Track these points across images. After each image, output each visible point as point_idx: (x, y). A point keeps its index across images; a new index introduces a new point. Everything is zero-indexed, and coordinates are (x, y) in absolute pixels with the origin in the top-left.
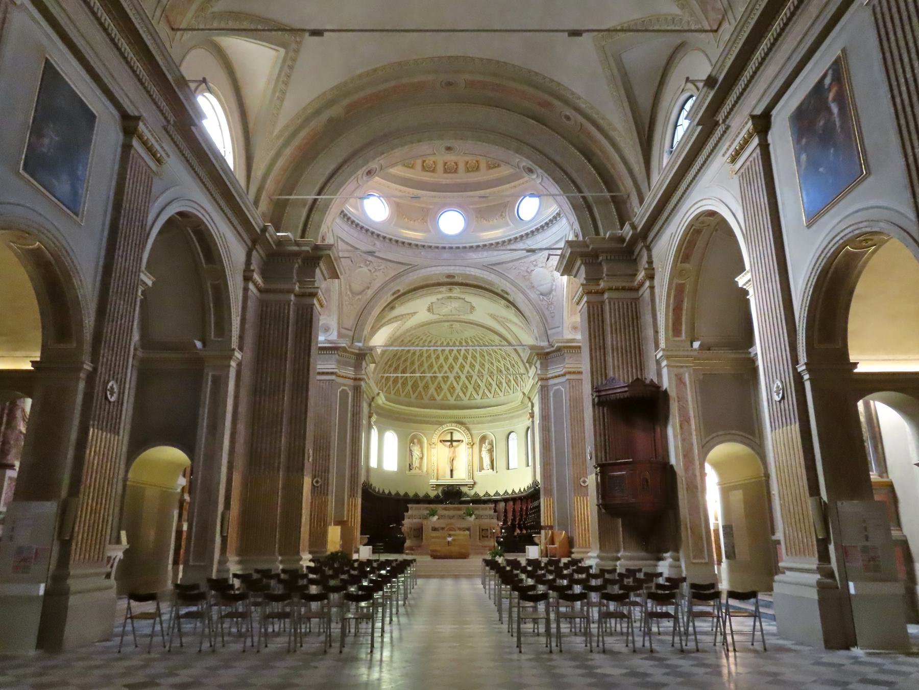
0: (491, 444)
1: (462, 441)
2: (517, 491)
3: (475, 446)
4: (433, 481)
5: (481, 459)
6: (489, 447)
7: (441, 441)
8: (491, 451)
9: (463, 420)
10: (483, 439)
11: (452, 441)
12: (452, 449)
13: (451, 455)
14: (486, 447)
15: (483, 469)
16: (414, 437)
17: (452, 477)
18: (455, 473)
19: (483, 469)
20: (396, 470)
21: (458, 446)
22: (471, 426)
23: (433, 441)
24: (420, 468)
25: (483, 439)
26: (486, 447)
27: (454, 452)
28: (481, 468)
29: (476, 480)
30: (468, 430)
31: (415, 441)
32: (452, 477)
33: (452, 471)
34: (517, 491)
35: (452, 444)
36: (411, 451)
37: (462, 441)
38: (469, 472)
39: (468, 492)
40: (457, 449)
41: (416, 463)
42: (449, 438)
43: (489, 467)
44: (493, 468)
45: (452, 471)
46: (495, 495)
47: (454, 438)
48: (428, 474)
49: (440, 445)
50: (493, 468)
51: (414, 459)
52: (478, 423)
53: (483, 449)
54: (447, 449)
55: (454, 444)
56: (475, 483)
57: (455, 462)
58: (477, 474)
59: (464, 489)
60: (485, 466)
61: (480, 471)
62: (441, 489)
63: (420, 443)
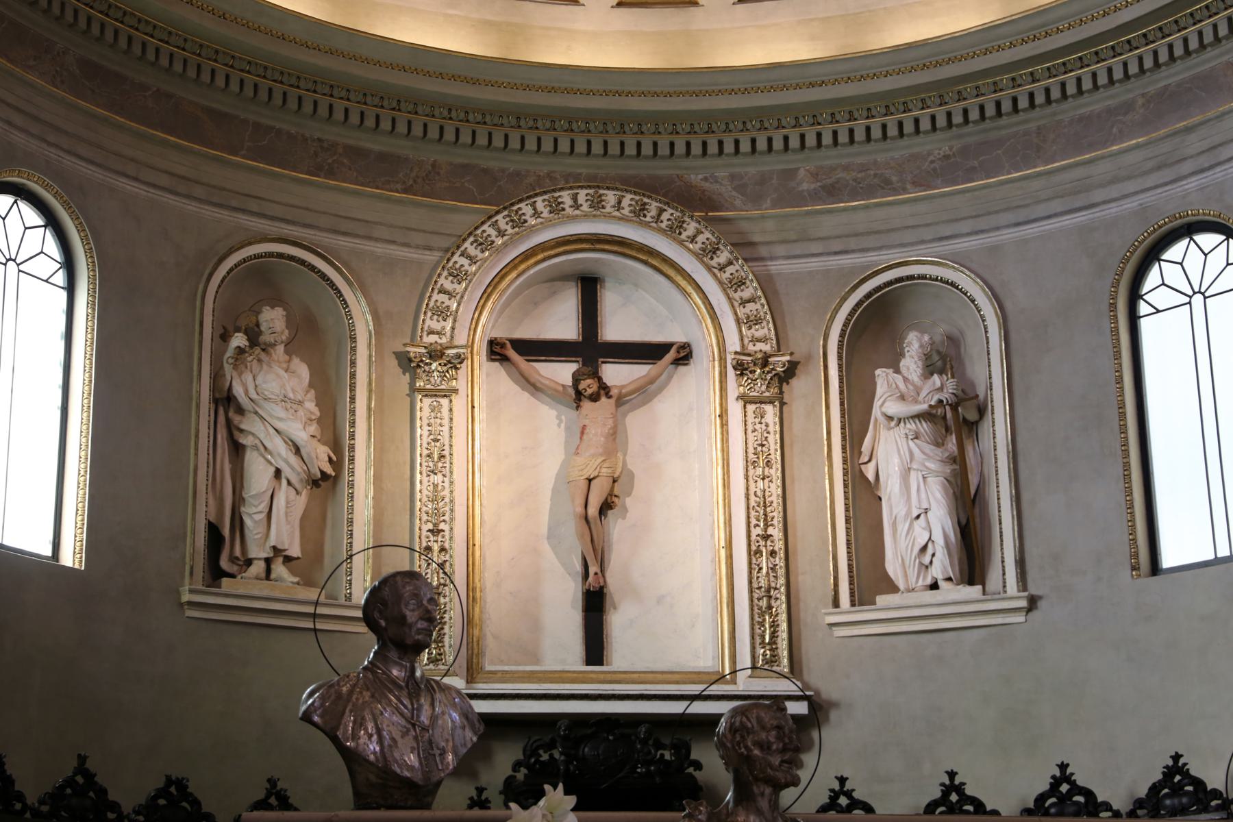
1: (684, 355)
3: (798, 385)
7: (496, 350)
9: (696, 174)
12: (598, 414)
13: (589, 463)
15: (891, 587)
17: (595, 649)
18: (617, 622)
19: (891, 587)
20: (69, 557)
21: (644, 393)
27: (616, 437)
30: (745, 247)
31: (273, 320)
32: (595, 649)
36: (225, 401)
37: (684, 355)
40: (635, 421)
43: (941, 566)
47: (614, 329)
51: (258, 475)
52: (832, 192)
53: (886, 403)
55: (616, 374)
56: (819, 710)
57: (618, 529)
61: (861, 598)
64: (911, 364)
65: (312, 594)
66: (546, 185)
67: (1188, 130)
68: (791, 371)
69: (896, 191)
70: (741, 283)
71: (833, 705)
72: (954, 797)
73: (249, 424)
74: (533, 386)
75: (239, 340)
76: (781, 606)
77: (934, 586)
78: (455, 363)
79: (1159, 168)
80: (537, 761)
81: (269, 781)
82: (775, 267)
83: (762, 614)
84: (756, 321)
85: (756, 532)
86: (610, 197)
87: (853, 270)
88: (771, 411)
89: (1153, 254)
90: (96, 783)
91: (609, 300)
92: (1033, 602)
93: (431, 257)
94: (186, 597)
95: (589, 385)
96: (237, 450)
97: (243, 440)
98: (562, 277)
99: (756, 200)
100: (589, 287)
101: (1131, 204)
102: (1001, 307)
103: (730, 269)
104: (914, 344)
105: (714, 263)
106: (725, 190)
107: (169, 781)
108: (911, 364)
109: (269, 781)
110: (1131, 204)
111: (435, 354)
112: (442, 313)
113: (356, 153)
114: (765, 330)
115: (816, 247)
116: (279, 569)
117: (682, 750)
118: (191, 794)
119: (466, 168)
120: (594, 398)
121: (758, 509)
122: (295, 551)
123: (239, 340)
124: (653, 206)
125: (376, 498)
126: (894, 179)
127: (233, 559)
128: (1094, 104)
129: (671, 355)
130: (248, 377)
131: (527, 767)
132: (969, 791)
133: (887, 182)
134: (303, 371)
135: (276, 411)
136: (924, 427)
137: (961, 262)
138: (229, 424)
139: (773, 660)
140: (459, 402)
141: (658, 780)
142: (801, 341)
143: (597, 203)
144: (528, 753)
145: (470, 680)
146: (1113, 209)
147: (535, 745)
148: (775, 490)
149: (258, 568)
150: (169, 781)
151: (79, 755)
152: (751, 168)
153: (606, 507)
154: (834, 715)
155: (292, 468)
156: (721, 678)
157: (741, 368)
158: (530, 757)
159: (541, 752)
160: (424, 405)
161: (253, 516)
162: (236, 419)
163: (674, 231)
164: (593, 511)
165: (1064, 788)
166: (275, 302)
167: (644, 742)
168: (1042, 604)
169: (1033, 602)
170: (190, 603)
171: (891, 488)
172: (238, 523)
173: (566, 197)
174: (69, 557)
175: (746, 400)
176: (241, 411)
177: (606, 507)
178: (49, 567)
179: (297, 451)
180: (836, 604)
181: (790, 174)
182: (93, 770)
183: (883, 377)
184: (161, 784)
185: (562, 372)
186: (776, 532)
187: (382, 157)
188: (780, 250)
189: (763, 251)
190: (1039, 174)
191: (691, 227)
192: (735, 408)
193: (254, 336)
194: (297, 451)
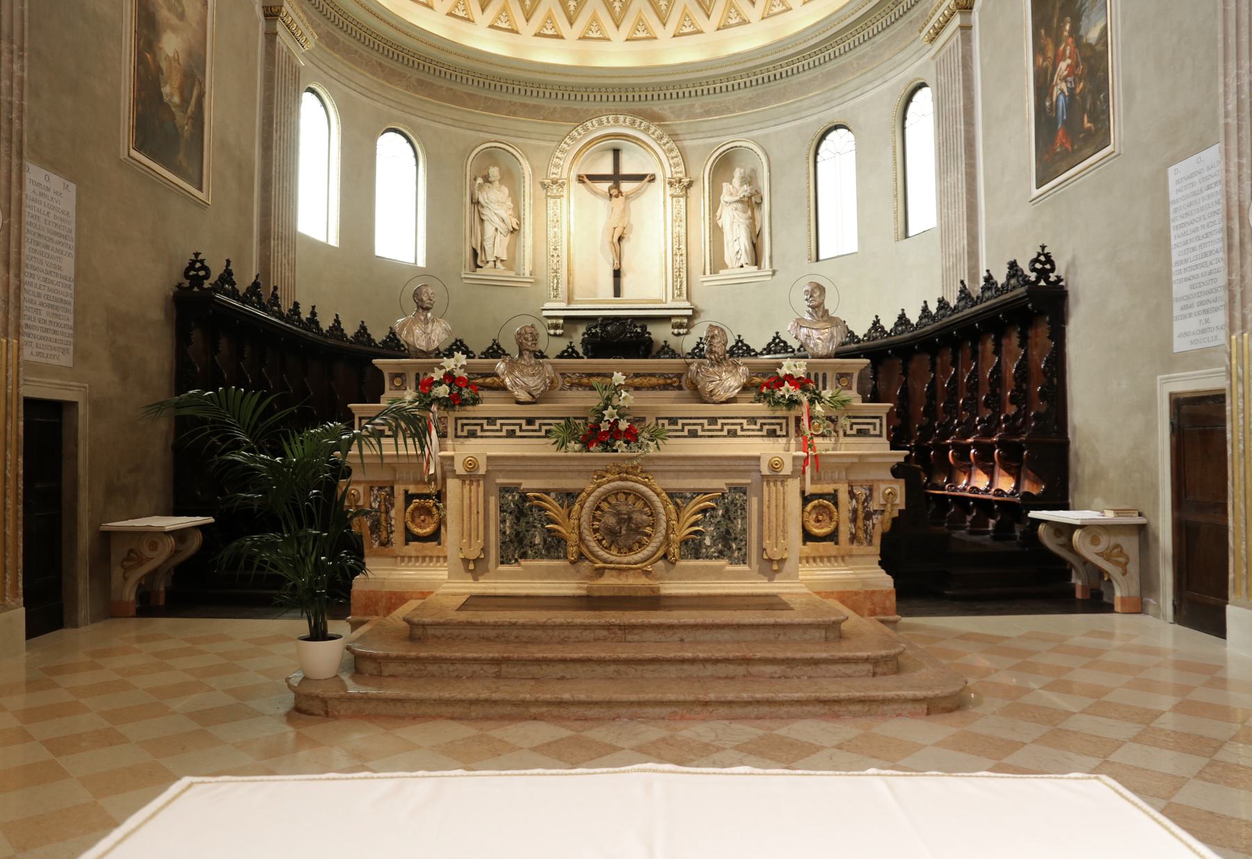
0: (750, 179)
1: (653, 179)
2: (888, 324)
3: (693, 190)
4: (557, 306)
5: (716, 232)
6: (745, 190)
7: (580, 179)
8: (752, 203)
9: (657, 107)
10: (724, 164)
11: (617, 178)
14: (733, 189)
15: (725, 266)
16: (490, 156)
17: (617, 292)
18: (626, 281)
19: (725, 266)
20: (422, 263)
21: (637, 193)
22: (680, 125)
23: (554, 173)
24: (511, 262)
25: (724, 164)
26: (733, 189)
27: (625, 211)
28: (717, 264)
29: (698, 302)
30: (674, 136)
31: (494, 172)
32: (617, 292)
33: (617, 274)
34: (888, 324)
35: (617, 186)
36: (476, 203)
37: (653, 179)
38: (676, 276)
39: (673, 342)
40: (633, 205)
41: (497, 247)
42: (606, 168)
43: (744, 259)
44: (757, 261)
45: (617, 274)
46: (768, 350)
47: (625, 170)
48: (536, 283)
49: (575, 185)
50: (757, 261)
51: (489, 230)
52: (708, 113)
53: (725, 197)
54: (602, 205)
55: (626, 187)
56: (696, 312)
58: (704, 282)
59: (660, 333)
60: (729, 257)
61: (714, 271)
62: (582, 329)
63: (511, 179)
64: (736, 181)
65: (512, 274)
66: (597, 115)
67: (835, 88)
68: (690, 184)
69: (731, 112)
70: (672, 150)
71: (702, 311)
72: (740, 344)
73: (484, 211)
74: (595, 193)
75: (480, 180)
76: (684, 275)
77: (742, 266)
78: (562, 185)
79: (826, 103)
82: (686, 143)
83: (677, 278)
84: (677, 165)
85: (675, 247)
86: (621, 118)
87: (715, 144)
88: (682, 201)
89: (823, 137)
91: (624, 158)
92: (774, 273)
93: (555, 144)
94: (463, 276)
95: (614, 192)
96: (482, 221)
97: (483, 218)
98: (606, 150)
99: (679, 117)
100: (616, 152)
101: (815, 117)
102: (768, 158)
103: (668, 145)
104: (738, 173)
105: (661, 143)
106: (667, 113)
107: (457, 340)
108: (736, 181)
110: (815, 117)
111: (555, 182)
112: (557, 166)
113: (524, 105)
114: (682, 168)
115: (701, 135)
116: (499, 264)
117: (644, 328)
119: (566, 109)
120: (617, 196)
121: (676, 238)
122: (504, 258)
123: (480, 180)
124: (638, 121)
125: (533, 238)
126: (731, 107)
127: (482, 261)
128: (804, 77)
129: (648, 178)
130: (484, 194)
132: (745, 342)
133: (728, 108)
134: (506, 190)
135: (494, 207)
136: (739, 206)
137: (754, 140)
138: (479, 211)
139: (680, 295)
140: (564, 200)
142: (693, 175)
143: (616, 121)
145: (569, 303)
146: (809, 120)
148: (683, 231)
149: (491, 264)
150: (457, 340)
152: (678, 104)
153: (620, 239)
154: (702, 314)
155: (502, 228)
156: (661, 301)
157: (671, 184)
160: (551, 201)
161: (488, 246)
162: (481, 209)
163: (647, 130)
164: (616, 240)
165: (777, 340)
166: (495, 164)
167: (630, 325)
168: (777, 273)
169: (774, 273)
171: (727, 230)
172: (483, 248)
173: (604, 119)
174: (422, 263)
175: (673, 196)
176: (482, 207)
177: (620, 239)
178: (413, 268)
179: (503, 221)
180: (704, 274)
181: (692, 106)
183: (725, 186)
184: (454, 341)
185: (604, 186)
186: (683, 247)
187: (535, 106)
188: (688, 137)
189: (681, 137)
190: (784, 105)
191: (653, 129)
192: (669, 199)
193: (487, 179)
194: (503, 221)
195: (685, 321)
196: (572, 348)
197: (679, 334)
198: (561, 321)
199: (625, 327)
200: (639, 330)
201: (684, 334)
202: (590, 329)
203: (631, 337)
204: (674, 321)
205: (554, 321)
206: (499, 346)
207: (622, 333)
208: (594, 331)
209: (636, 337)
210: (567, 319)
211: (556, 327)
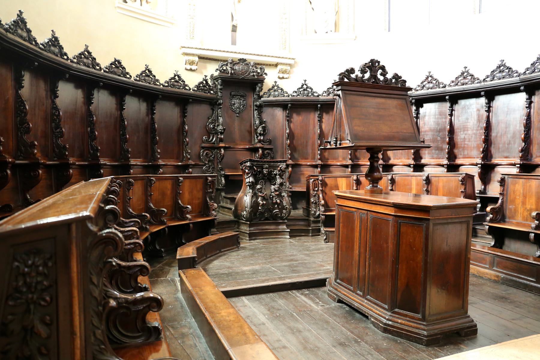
17: (234, 43)
32: (234, 43)
77: (327, 32)
80: (222, 69)
81: (146, 65)
90: (92, 55)
107: (116, 60)
109: (146, 65)
118: (122, 65)
131: (220, 71)
141: (256, 77)
144: (220, 66)
147: (222, 64)
150: (116, 60)
151: (86, 45)
158: (221, 67)
159: (224, 66)
170: (119, 7)
182: (91, 51)
184: (113, 60)
195: (288, 68)
196: (206, 81)
197: (283, 78)
198: (196, 59)
199: (249, 68)
200: (259, 71)
201: (286, 78)
202: (222, 66)
203: (254, 76)
204: (279, 67)
205: (192, 58)
206: (150, 72)
207: (247, 71)
208: (225, 68)
209: (257, 76)
210: (201, 58)
211: (192, 63)
